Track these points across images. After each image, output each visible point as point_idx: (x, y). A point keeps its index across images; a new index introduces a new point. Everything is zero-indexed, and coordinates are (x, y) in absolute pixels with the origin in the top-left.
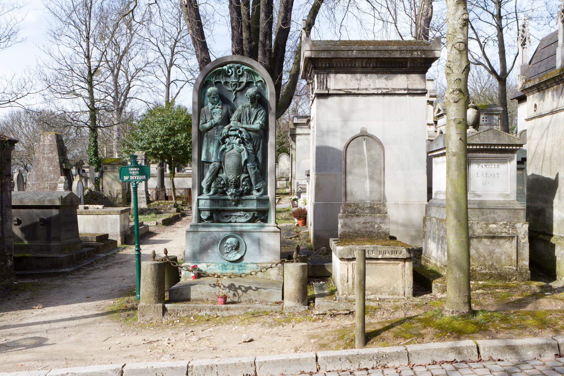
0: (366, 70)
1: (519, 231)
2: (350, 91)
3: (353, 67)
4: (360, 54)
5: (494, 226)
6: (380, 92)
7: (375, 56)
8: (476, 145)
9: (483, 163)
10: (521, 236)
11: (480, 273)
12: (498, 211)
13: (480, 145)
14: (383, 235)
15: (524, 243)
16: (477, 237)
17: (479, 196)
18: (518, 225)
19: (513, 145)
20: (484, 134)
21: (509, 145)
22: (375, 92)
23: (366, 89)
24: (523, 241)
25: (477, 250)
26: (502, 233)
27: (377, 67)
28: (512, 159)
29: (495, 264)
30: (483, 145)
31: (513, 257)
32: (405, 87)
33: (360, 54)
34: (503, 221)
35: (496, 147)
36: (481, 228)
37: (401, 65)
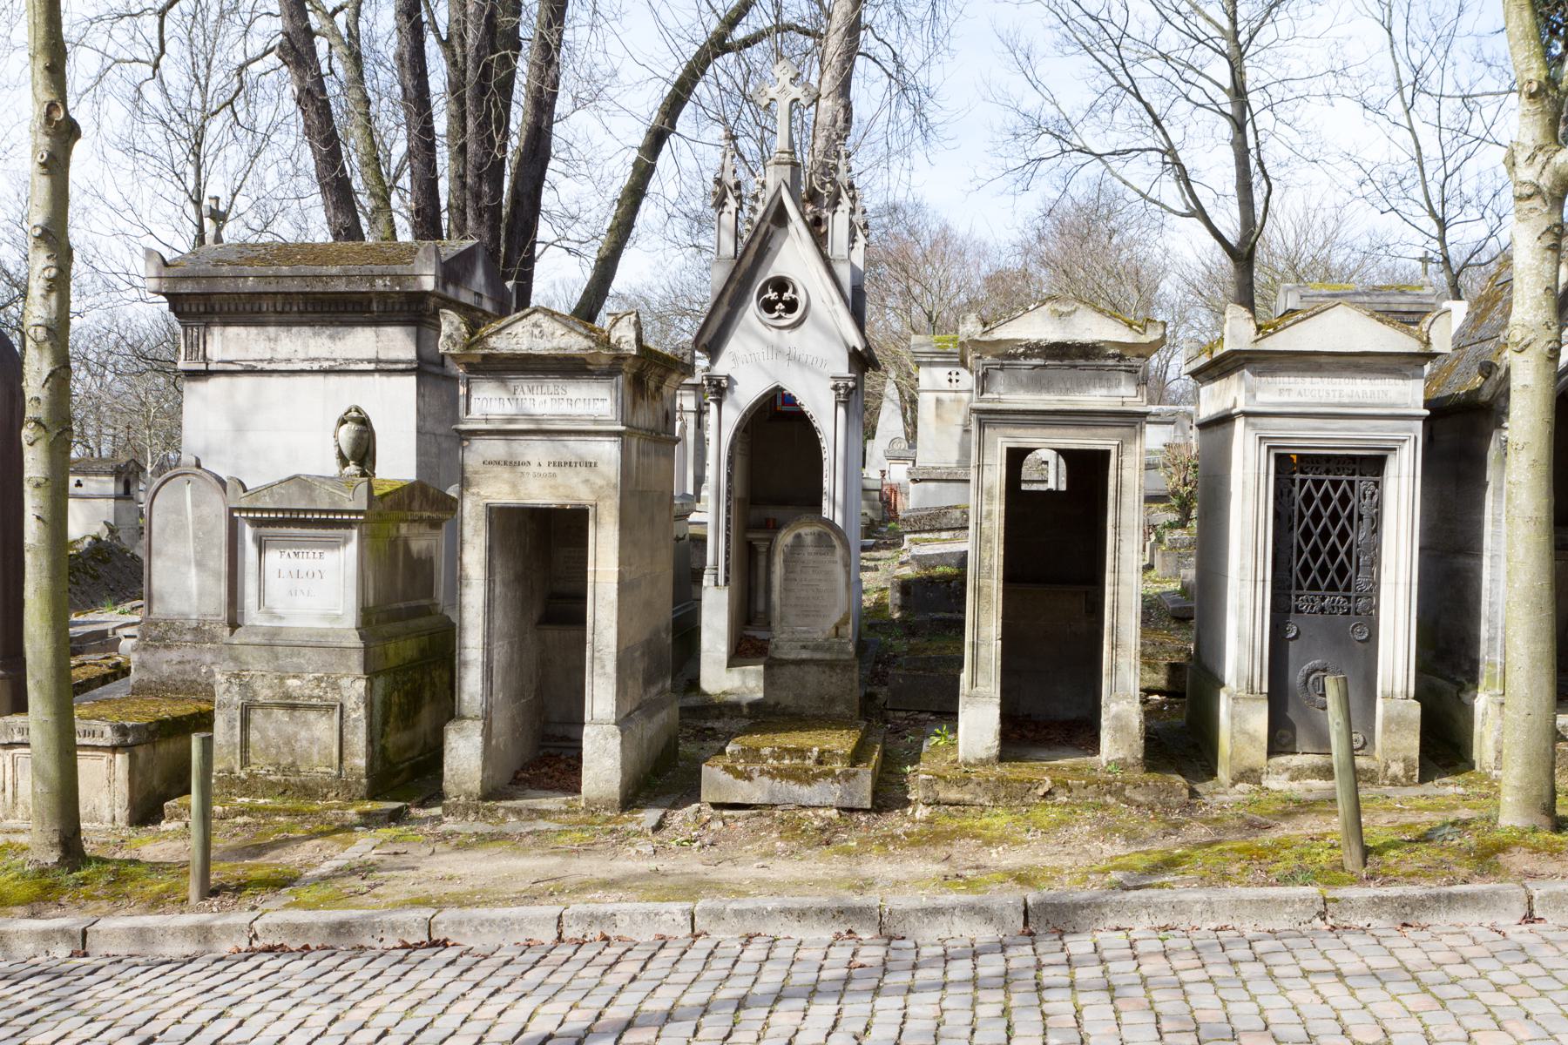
0: (285, 318)
1: (346, 694)
6: (316, 366)
7: (294, 290)
8: (269, 511)
10: (349, 705)
12: (306, 650)
13: (276, 511)
15: (356, 720)
16: (262, 706)
17: (281, 618)
18: (345, 682)
19: (342, 512)
21: (335, 512)
22: (306, 366)
24: (354, 716)
26: (311, 697)
27: (306, 311)
28: (346, 541)
30: (283, 511)
32: (372, 355)
36: (270, 687)
37: (357, 308)
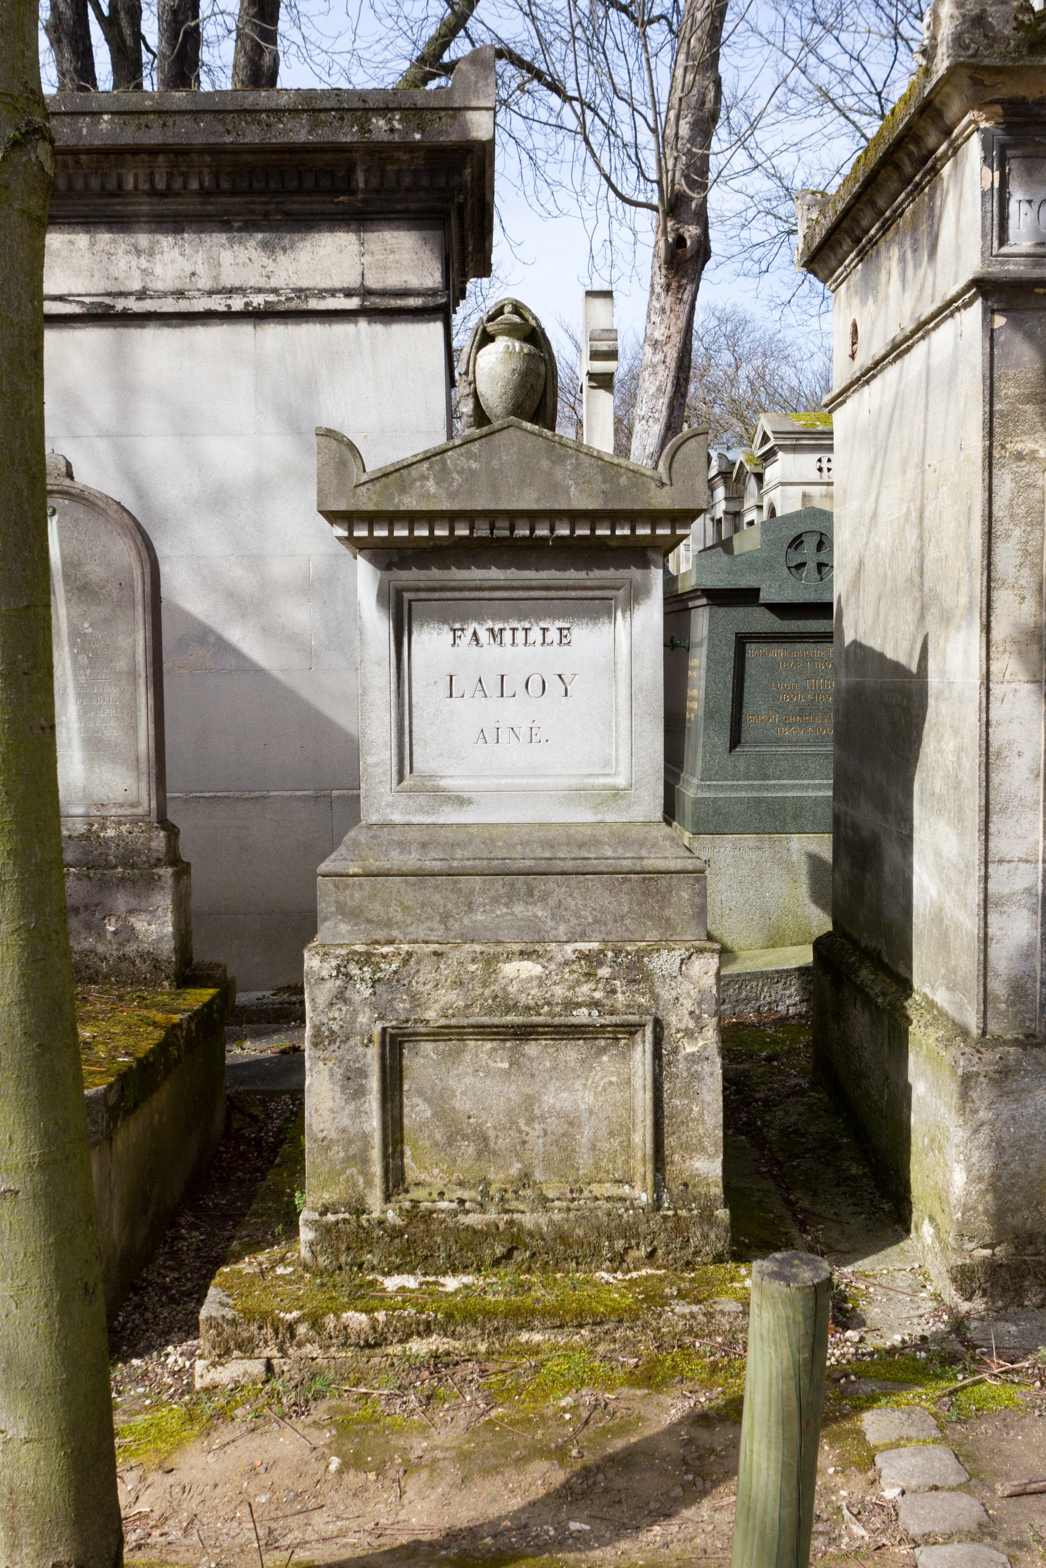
0: (172, 206)
1: (665, 994)
2: (107, 300)
3: (112, 195)
4: (131, 129)
5: (530, 968)
6: (237, 304)
7: (199, 140)
8: (431, 518)
9: (480, 618)
10: (677, 1020)
11: (457, 1231)
12: (551, 881)
13: (451, 517)
14: (144, 967)
15: (693, 1059)
16: (438, 1034)
17: (461, 801)
18: (664, 962)
19: (633, 517)
20: (470, 455)
21: (614, 517)
22: (217, 303)
23: (180, 294)
24: (690, 1048)
25: (440, 1102)
26: (570, 1005)
27: (216, 191)
28: (635, 596)
29: (538, 1176)
30: (470, 517)
31: (637, 1138)
32: (352, 280)
33: (131, 129)
34: (583, 937)
35: (542, 532)
36: (459, 984)
37: (325, 183)
